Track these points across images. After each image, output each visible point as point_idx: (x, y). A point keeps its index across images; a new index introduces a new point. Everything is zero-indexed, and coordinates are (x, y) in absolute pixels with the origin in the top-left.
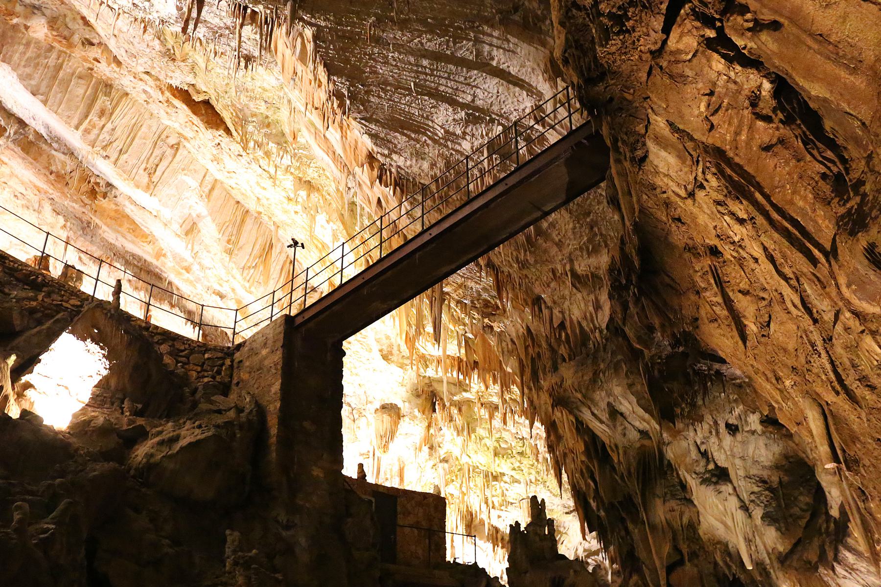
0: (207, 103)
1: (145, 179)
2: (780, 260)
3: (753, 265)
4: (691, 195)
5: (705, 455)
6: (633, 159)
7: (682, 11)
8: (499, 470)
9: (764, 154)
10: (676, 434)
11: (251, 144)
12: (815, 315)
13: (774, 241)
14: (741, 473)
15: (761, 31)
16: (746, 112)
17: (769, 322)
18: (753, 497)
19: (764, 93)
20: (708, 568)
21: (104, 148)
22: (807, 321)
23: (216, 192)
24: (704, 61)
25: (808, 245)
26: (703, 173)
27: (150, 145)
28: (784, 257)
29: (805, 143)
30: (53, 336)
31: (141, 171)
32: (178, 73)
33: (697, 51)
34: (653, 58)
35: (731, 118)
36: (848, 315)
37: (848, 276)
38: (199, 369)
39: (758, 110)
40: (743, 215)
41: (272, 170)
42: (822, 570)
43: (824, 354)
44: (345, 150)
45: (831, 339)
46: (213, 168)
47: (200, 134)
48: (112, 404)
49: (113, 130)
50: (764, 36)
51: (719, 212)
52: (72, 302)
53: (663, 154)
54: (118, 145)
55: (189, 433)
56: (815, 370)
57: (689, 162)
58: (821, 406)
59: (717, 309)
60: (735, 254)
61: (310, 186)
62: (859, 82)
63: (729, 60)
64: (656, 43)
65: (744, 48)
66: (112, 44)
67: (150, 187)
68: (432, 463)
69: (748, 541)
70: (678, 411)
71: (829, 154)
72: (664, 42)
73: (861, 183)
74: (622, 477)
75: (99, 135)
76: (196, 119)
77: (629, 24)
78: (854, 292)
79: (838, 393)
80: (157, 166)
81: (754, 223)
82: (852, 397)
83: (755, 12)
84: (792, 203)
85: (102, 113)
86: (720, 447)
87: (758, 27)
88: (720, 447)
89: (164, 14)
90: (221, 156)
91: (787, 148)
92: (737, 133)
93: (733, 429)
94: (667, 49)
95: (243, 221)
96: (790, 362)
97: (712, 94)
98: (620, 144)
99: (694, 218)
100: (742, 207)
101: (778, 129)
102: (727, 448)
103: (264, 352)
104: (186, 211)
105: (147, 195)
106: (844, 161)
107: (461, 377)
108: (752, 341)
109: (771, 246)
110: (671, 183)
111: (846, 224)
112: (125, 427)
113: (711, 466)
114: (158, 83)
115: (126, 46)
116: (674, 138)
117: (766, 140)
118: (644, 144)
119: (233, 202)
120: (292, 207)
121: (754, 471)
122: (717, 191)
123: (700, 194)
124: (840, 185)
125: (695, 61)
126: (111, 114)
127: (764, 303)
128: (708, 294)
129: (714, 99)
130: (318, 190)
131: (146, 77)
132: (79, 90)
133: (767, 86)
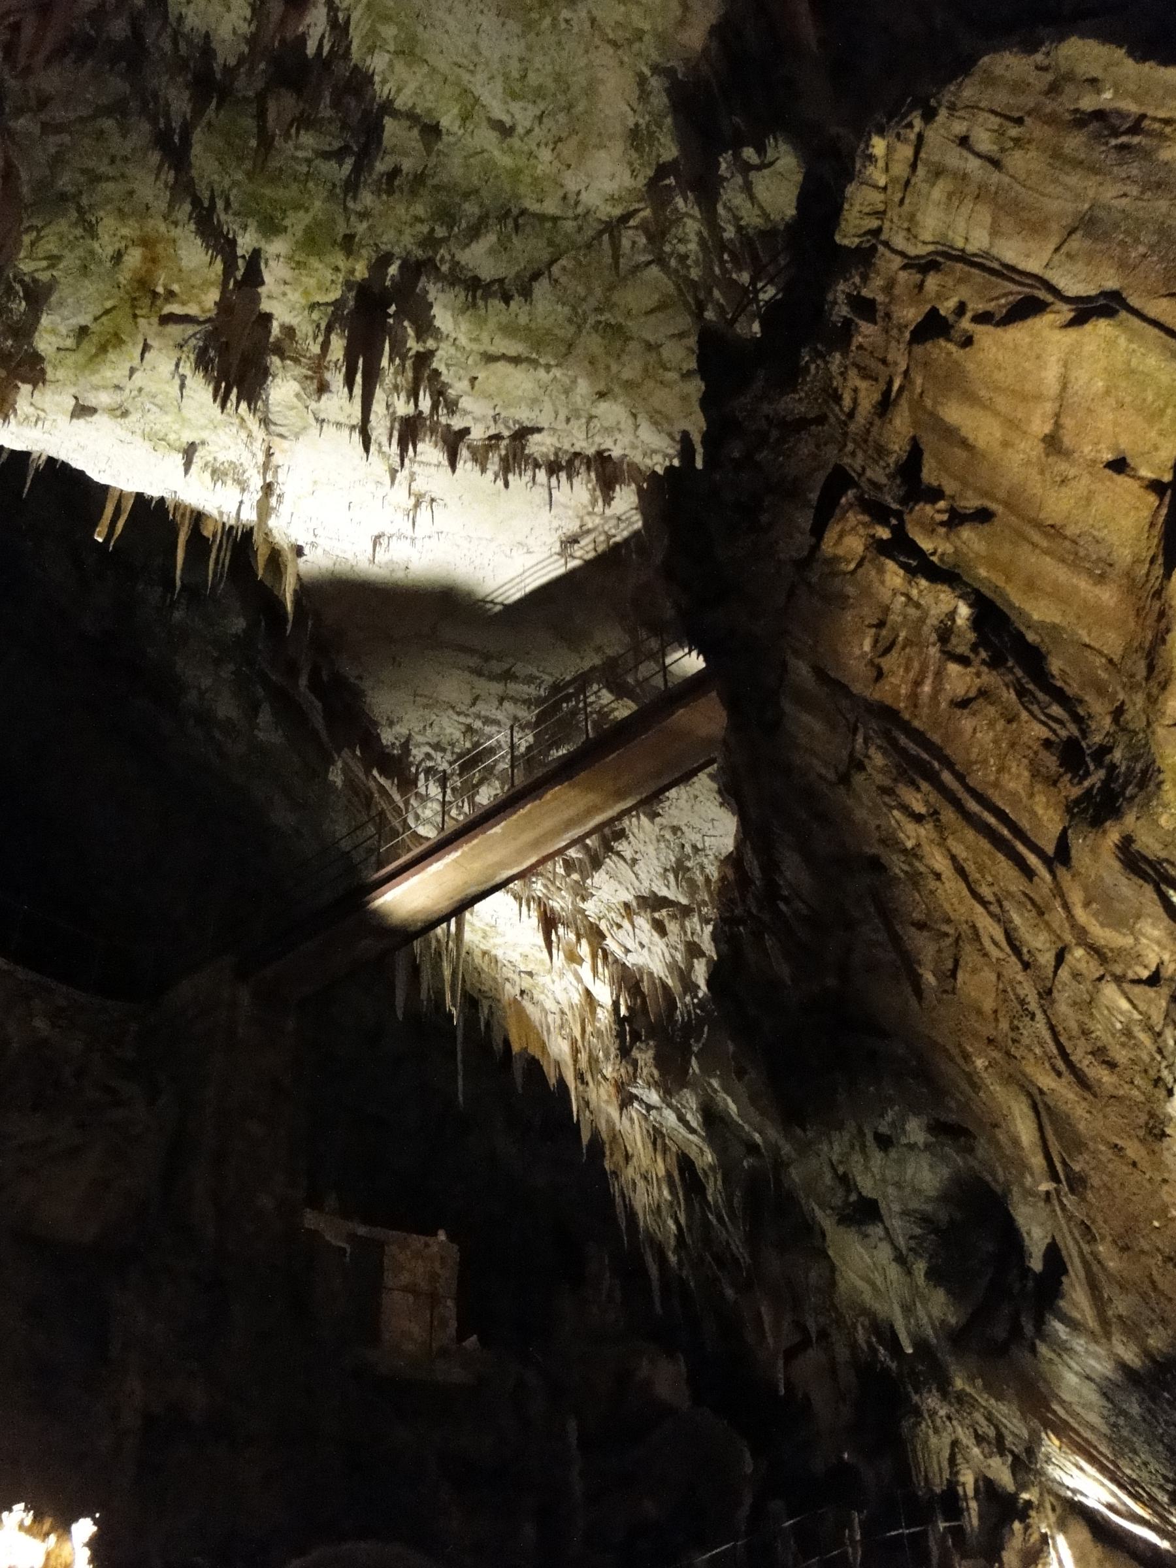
2: (975, 875)
4: (845, 779)
5: (845, 1180)
7: (843, 500)
9: (958, 712)
10: (804, 1149)
12: (1026, 957)
13: (968, 844)
14: (896, 1207)
15: (961, 523)
18: (913, 1243)
20: (842, 1354)
24: (873, 573)
25: (1021, 848)
29: (1021, 693)
33: (863, 559)
35: (910, 659)
36: (1079, 952)
37: (1086, 889)
39: (949, 647)
43: (1039, 1016)
45: (1050, 992)
50: (966, 533)
51: (885, 804)
53: (806, 718)
56: (1026, 1041)
58: (1030, 1095)
60: (906, 868)
62: (1107, 596)
63: (912, 572)
65: (933, 554)
69: (908, 1310)
71: (1056, 710)
72: (815, 548)
73: (1104, 750)
74: (720, 1218)
77: (764, 518)
78: (1095, 915)
79: (1059, 1074)
81: (938, 820)
82: (1082, 1081)
83: (953, 497)
84: (996, 785)
87: (956, 519)
88: (867, 1168)
91: (992, 704)
93: (885, 1142)
96: (987, 1030)
97: (881, 624)
100: (919, 796)
108: (930, 997)
110: (815, 761)
111: (1085, 810)
113: (853, 1197)
121: (914, 1205)
123: (859, 778)
124: (1072, 755)
125: (860, 571)
129: (884, 632)
133: (964, 611)
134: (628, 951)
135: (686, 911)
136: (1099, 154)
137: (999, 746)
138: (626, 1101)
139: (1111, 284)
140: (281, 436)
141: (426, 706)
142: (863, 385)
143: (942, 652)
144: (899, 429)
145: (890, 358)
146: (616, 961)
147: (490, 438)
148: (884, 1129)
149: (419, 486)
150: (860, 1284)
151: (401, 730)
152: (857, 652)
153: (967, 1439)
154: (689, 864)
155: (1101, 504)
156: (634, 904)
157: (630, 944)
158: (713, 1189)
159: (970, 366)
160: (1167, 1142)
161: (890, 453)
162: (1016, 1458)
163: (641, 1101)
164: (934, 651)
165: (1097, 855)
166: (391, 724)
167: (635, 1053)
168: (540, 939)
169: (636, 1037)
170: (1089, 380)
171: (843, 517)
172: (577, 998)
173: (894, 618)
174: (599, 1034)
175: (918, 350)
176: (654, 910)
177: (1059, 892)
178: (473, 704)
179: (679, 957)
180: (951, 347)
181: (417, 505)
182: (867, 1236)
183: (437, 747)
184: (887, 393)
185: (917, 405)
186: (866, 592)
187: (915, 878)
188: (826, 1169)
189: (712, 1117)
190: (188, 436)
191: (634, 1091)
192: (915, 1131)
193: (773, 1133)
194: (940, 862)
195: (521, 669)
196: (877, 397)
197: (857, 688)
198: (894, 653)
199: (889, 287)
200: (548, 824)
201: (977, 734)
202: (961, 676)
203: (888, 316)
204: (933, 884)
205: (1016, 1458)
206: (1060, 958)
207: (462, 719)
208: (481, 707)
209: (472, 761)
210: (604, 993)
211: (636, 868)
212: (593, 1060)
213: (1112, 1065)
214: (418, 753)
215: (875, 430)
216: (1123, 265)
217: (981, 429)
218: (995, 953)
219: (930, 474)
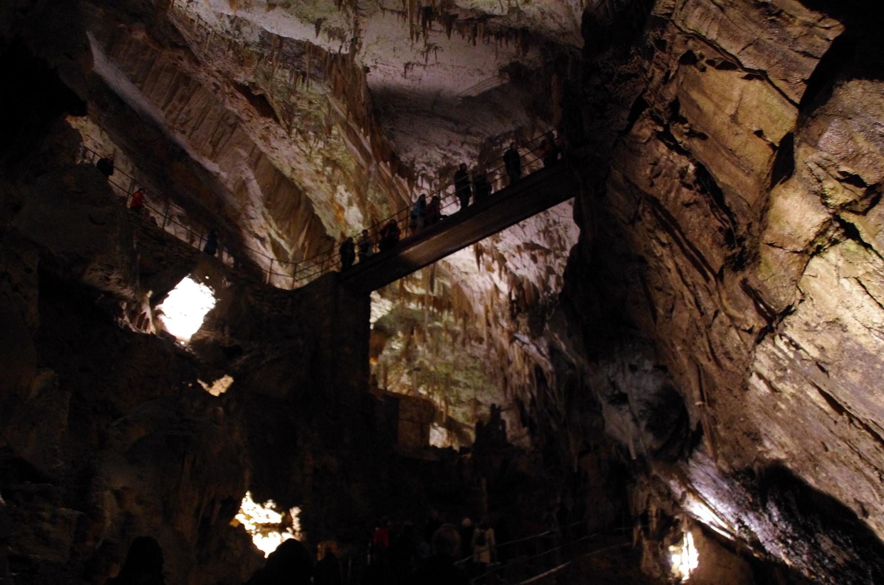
0: (263, 97)
1: (210, 150)
2: (685, 273)
4: (632, 222)
5: (614, 385)
8: (456, 378)
9: (685, 208)
11: (295, 130)
12: (702, 310)
13: (682, 260)
14: (636, 397)
15: (693, 137)
16: (676, 181)
19: (689, 171)
21: (182, 125)
22: (696, 314)
23: (262, 162)
24: (654, 145)
25: (706, 269)
28: (688, 271)
29: (712, 207)
30: (178, 280)
31: (207, 144)
35: (666, 181)
36: (723, 314)
37: (728, 294)
39: (684, 180)
41: (308, 152)
42: (679, 462)
43: (705, 335)
45: (710, 326)
46: (260, 143)
47: (254, 120)
49: (190, 111)
53: (617, 194)
54: (191, 123)
56: (698, 344)
58: (697, 366)
61: (335, 164)
62: (750, 181)
66: (194, 48)
67: (214, 157)
69: (635, 441)
71: (725, 216)
72: (630, 127)
73: (742, 239)
74: (553, 394)
75: (178, 115)
78: (731, 304)
79: (710, 360)
80: (219, 140)
84: (698, 240)
87: (692, 134)
91: (700, 208)
93: (633, 369)
96: (683, 336)
97: (655, 164)
106: (734, 223)
107: (435, 311)
108: (660, 320)
109: (680, 263)
111: (731, 263)
113: (616, 392)
114: (226, 79)
117: (687, 199)
121: (643, 397)
122: (650, 223)
123: (638, 224)
125: (648, 145)
126: (189, 99)
127: (670, 297)
129: (656, 168)
130: (341, 168)
131: (217, 74)
132: (166, 80)
133: (692, 167)
134: (517, 268)
136: (762, 21)
137: (700, 225)
138: (512, 339)
139: (764, 68)
140: (364, 16)
141: (424, 144)
142: (657, 71)
143: (681, 182)
146: (511, 273)
148: (634, 363)
149: (431, 40)
150: (616, 430)
151: (411, 155)
152: (643, 173)
154: (551, 229)
155: (750, 148)
156: (522, 247)
157: (519, 265)
158: (551, 381)
159: (703, 80)
160: (748, 392)
161: (666, 100)
163: (519, 340)
165: (734, 282)
166: (406, 152)
167: (519, 318)
168: (474, 259)
170: (751, 100)
171: (643, 120)
172: (489, 287)
173: (662, 164)
174: (500, 305)
175: (682, 67)
177: (717, 288)
178: (449, 145)
179: (542, 273)
181: (428, 51)
183: (429, 164)
186: (650, 152)
187: (659, 270)
188: (606, 381)
189: (553, 351)
190: (318, 15)
191: (517, 335)
192: (648, 365)
194: (670, 265)
195: (474, 129)
196: (663, 75)
197: (642, 187)
198: (660, 177)
199: (673, 38)
201: (693, 219)
202: (687, 193)
203: (671, 48)
204: (668, 274)
206: (716, 313)
207: (442, 151)
208: (452, 147)
210: (504, 287)
212: (496, 318)
213: (731, 359)
214: (418, 167)
215: (660, 90)
216: (768, 63)
217: (707, 106)
218: (690, 306)
219: (682, 112)
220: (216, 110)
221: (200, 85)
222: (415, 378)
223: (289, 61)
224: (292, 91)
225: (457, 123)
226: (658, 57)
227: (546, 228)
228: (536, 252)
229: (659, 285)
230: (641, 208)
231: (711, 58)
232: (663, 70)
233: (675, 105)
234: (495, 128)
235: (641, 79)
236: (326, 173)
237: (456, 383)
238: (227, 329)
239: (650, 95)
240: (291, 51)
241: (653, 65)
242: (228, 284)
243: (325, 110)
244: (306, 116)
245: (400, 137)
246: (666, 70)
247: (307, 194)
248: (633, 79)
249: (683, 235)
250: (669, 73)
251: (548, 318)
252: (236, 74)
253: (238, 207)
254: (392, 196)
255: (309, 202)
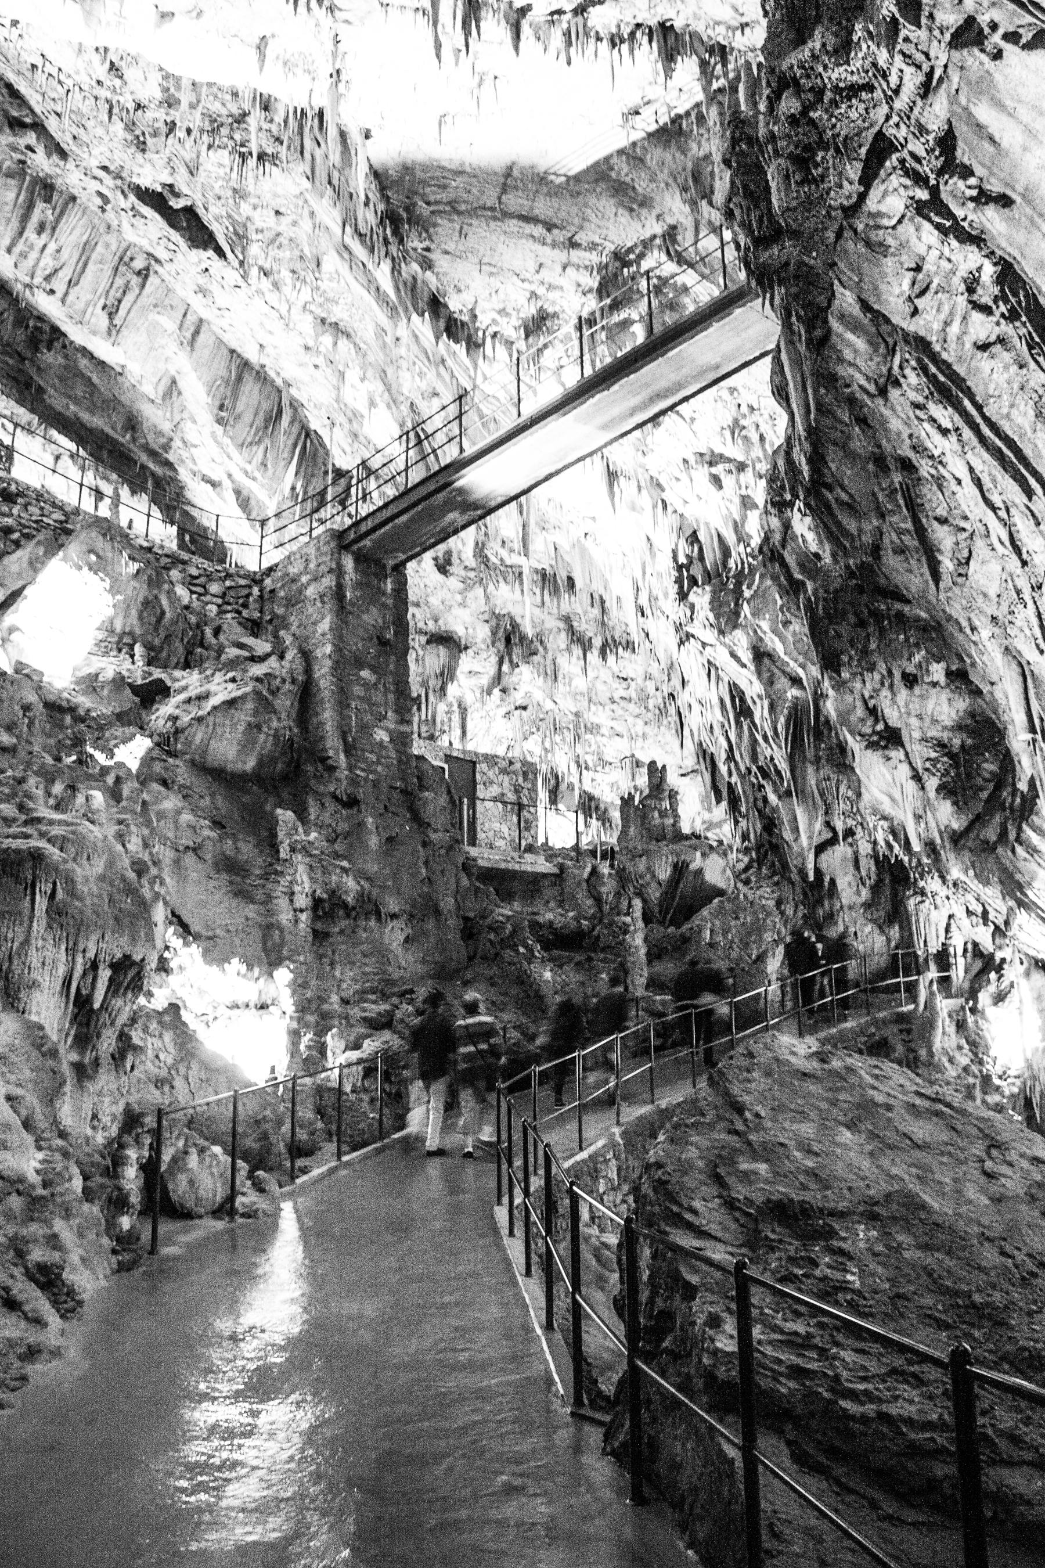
0: (190, 211)
1: (103, 321)
3: (953, 485)
4: (883, 392)
5: (873, 712)
6: (809, 342)
7: (888, 164)
8: (595, 720)
11: (254, 271)
12: (1025, 556)
14: (916, 735)
15: (986, 203)
17: (968, 559)
18: (928, 765)
20: (865, 848)
21: (48, 278)
22: (1014, 562)
23: (202, 338)
24: (912, 229)
26: (901, 367)
27: (108, 272)
28: (994, 481)
29: (1030, 348)
32: (148, 169)
33: (903, 216)
34: (846, 217)
38: (220, 601)
39: (975, 297)
40: (946, 424)
41: (284, 309)
42: (1000, 850)
44: (397, 289)
46: (198, 304)
47: (179, 255)
48: (120, 651)
49: (58, 251)
51: (918, 418)
52: (55, 516)
53: (850, 336)
54: (65, 275)
55: (220, 688)
56: (1018, 623)
57: (882, 350)
58: (1020, 665)
59: (906, 538)
60: (933, 471)
64: (849, 197)
66: (52, 125)
68: (503, 710)
70: (845, 658)
72: (862, 197)
74: (765, 738)
75: (39, 260)
76: (175, 236)
80: (120, 301)
84: (1008, 416)
85: (41, 229)
86: (893, 701)
87: (983, 198)
88: (893, 701)
89: (143, 97)
90: (209, 287)
92: (947, 324)
93: (910, 681)
94: (865, 209)
95: (240, 379)
97: (918, 269)
98: (794, 319)
99: (883, 421)
101: (998, 324)
102: (901, 703)
103: (304, 579)
104: (162, 366)
105: (109, 344)
108: (946, 582)
109: (978, 466)
110: (857, 375)
112: (139, 682)
113: (880, 727)
114: (119, 182)
115: (75, 130)
116: (865, 320)
118: (826, 321)
119: (226, 352)
120: (310, 359)
121: (932, 733)
122: (917, 390)
123: (894, 393)
125: (899, 228)
126: (54, 229)
128: (895, 519)
129: (920, 276)
130: (348, 336)
131: (101, 174)
133: (989, 270)
135: (741, 467)
140: (347, 22)
141: (491, 274)
142: (909, 70)
144: (936, 114)
145: (932, 54)
147: (552, 14)
148: (911, 669)
153: (960, 913)
156: (692, 460)
158: (760, 712)
159: (998, 77)
161: (928, 132)
162: (997, 927)
164: (962, 301)
167: (692, 597)
169: (694, 582)
173: (928, 267)
175: (956, 55)
176: (711, 464)
180: (984, 57)
182: (889, 759)
183: (502, 312)
184: (930, 75)
185: (953, 99)
187: (939, 482)
188: (859, 703)
189: (761, 655)
192: (938, 671)
193: (815, 671)
195: (581, 238)
196: (921, 78)
197: (896, 320)
198: (929, 295)
200: (616, 411)
202: (982, 324)
203: (931, 16)
205: (997, 927)
207: (526, 285)
209: (538, 324)
211: (694, 427)
212: (652, 599)
215: (916, 111)
219: (962, 155)
220: (107, 246)
221: (73, 199)
222: (518, 723)
223: (224, 131)
224: (239, 194)
225: (550, 227)
226: (907, 40)
227: (736, 421)
228: (719, 469)
229: (942, 511)
230: (897, 361)
231: (1011, 29)
232: (919, 67)
233: (947, 142)
234: (623, 230)
235: (878, 94)
236: (322, 349)
237: (594, 729)
238: (138, 649)
239: (897, 125)
240: (224, 112)
241: (898, 58)
242: (133, 567)
243: (306, 225)
244: (273, 241)
245: (442, 262)
246: (926, 67)
247: (293, 391)
248: (864, 95)
249: (979, 408)
250: (930, 75)
251: (747, 593)
252: (136, 170)
253: (166, 427)
254: (443, 380)
255: (295, 406)
